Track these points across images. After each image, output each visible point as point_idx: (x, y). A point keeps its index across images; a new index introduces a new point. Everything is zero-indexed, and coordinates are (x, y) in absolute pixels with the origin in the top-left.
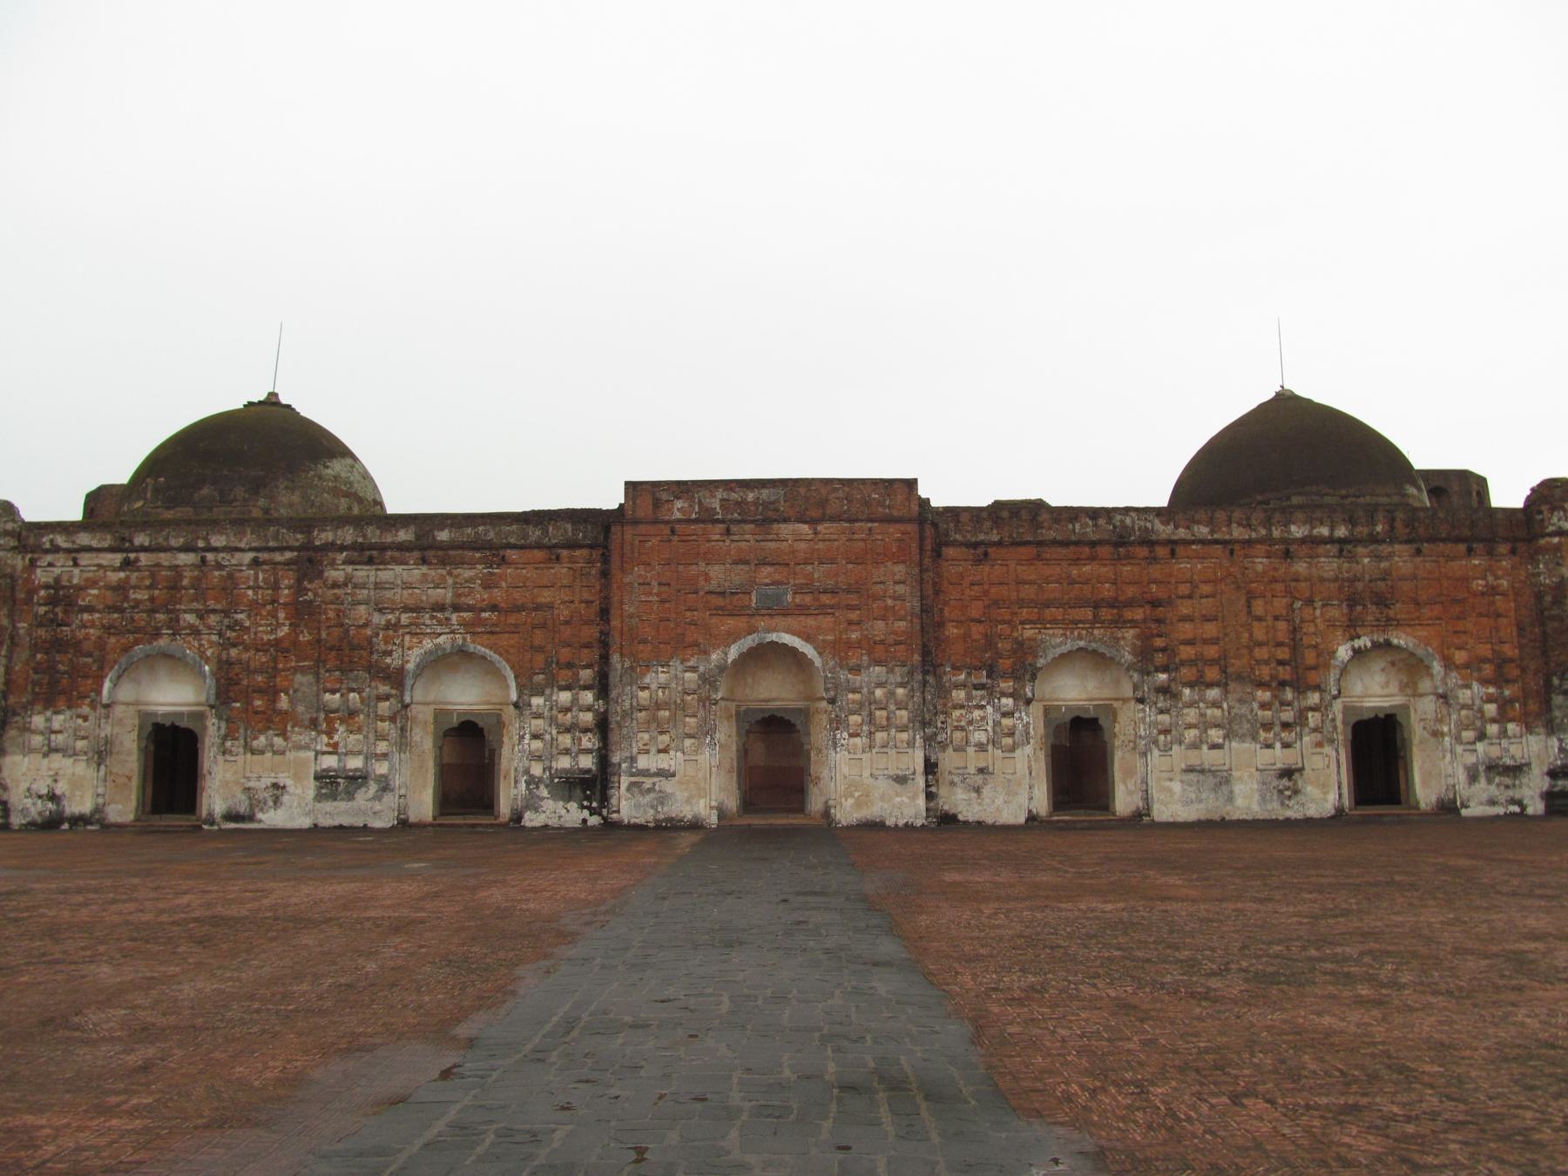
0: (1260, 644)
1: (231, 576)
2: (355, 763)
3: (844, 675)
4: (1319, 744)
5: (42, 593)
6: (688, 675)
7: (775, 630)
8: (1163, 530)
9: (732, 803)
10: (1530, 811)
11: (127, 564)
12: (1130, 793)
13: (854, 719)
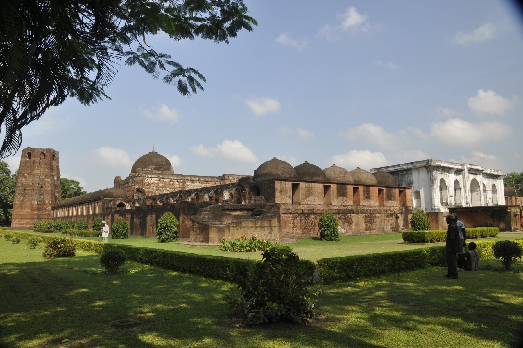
11: (159, 180)
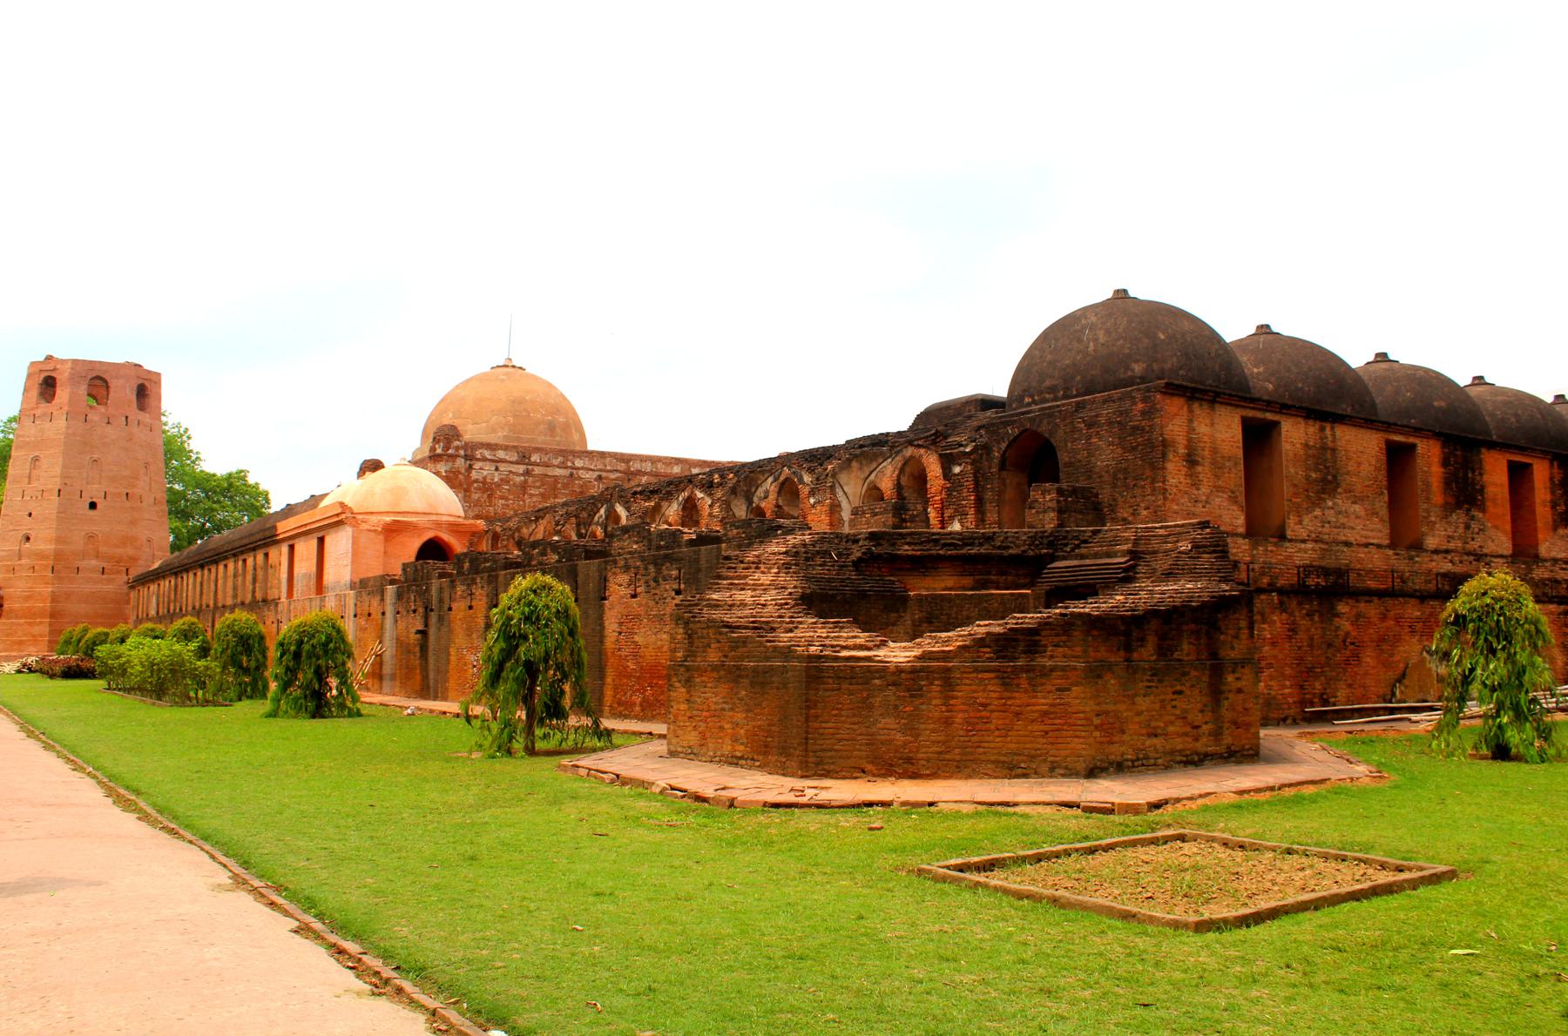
11: (527, 473)
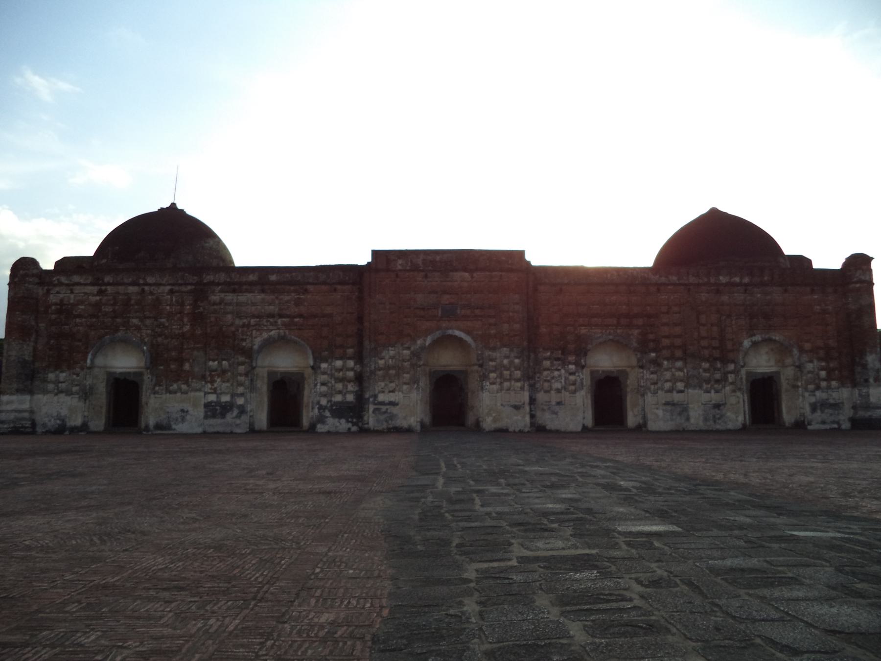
0: (704, 338)
1: (158, 299)
2: (225, 398)
3: (487, 353)
4: (734, 391)
5: (53, 307)
6: (405, 352)
7: (451, 328)
8: (654, 278)
9: (427, 420)
10: (843, 427)
11: (101, 292)
12: (635, 416)
13: (493, 375)
